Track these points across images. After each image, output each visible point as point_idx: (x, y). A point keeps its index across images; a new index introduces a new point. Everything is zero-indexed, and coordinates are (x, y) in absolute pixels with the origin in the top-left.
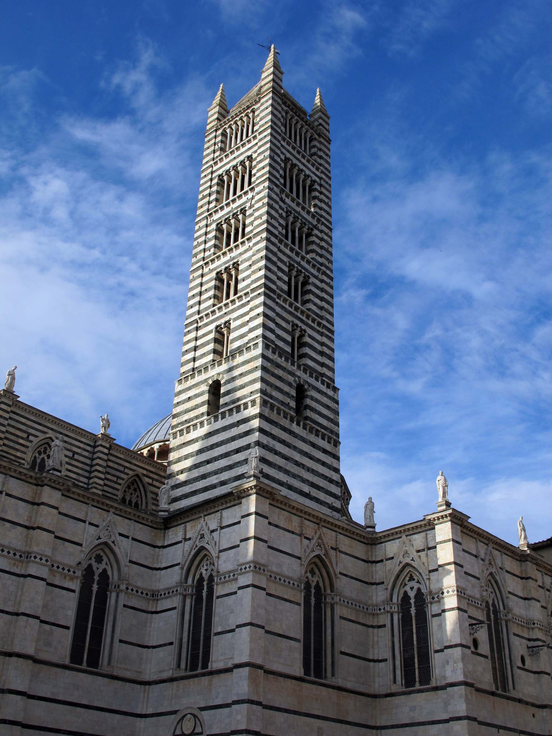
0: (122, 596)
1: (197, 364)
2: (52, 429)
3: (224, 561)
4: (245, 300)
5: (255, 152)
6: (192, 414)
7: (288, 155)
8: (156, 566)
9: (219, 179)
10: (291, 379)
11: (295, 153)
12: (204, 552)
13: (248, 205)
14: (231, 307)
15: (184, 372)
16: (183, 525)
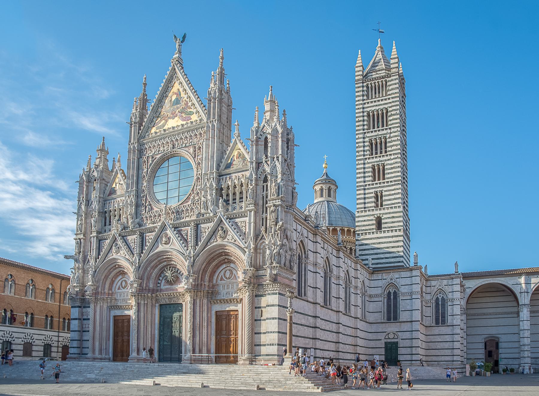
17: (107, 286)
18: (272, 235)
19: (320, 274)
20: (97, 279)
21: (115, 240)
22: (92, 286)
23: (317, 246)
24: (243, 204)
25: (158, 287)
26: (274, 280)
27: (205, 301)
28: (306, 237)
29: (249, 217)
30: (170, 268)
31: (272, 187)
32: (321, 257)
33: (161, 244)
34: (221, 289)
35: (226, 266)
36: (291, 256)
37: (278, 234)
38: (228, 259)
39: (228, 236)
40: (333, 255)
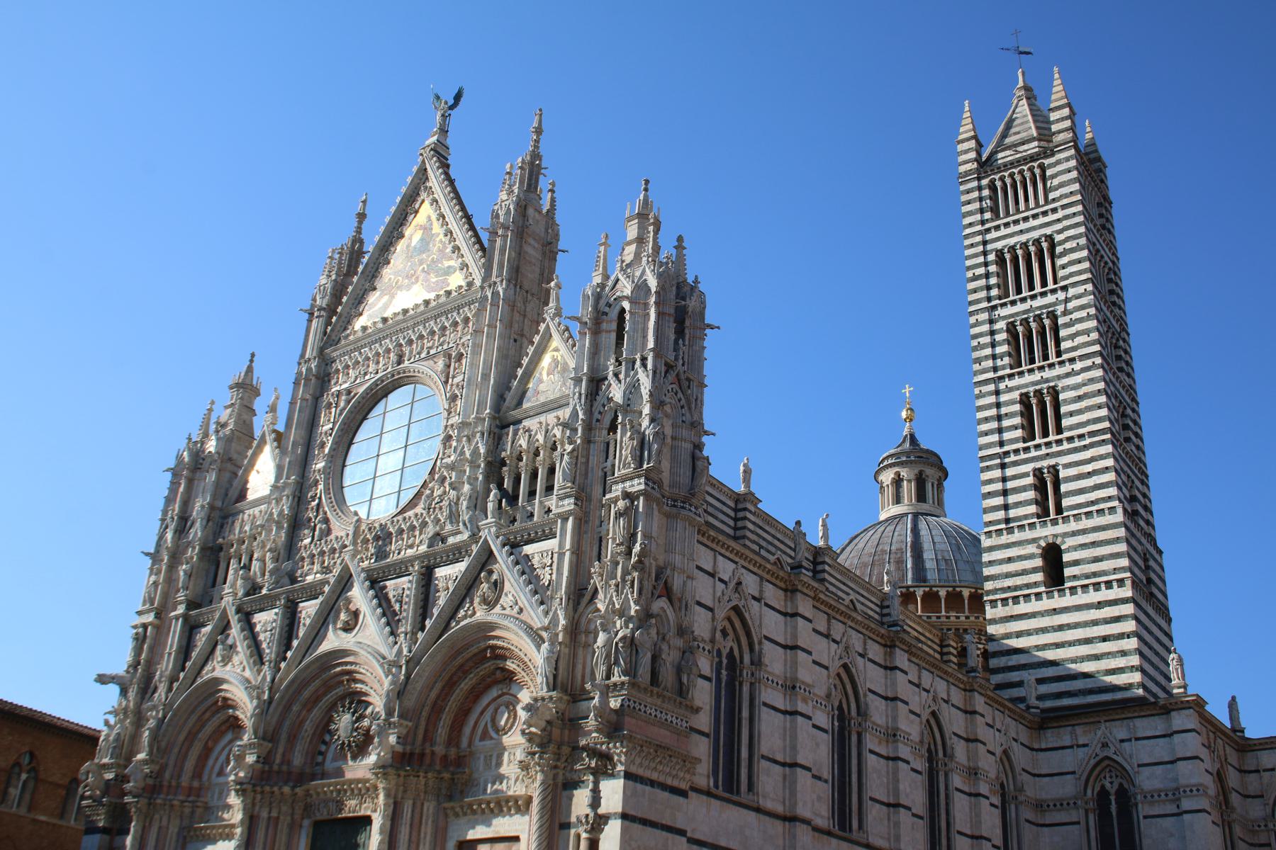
0: (1022, 808)
1: (1012, 513)
2: (852, 589)
3: (1148, 778)
4: (1077, 444)
5: (1060, 232)
6: (1019, 581)
7: (1095, 240)
8: (1036, 772)
9: (997, 256)
10: (1139, 548)
11: (1095, 231)
12: (1107, 762)
13: (1060, 309)
14: (1055, 449)
15: (990, 522)
16: (1070, 728)
17: (189, 765)
18: (617, 586)
19: (809, 718)
20: (163, 744)
21: (224, 627)
22: (147, 764)
23: (795, 628)
24: (552, 502)
25: (318, 764)
26: (613, 726)
27: (429, 807)
28: (754, 598)
29: (561, 535)
30: (351, 703)
31: (624, 443)
32: (814, 662)
33: (335, 629)
34: (481, 768)
35: (500, 692)
36: (684, 652)
37: (633, 582)
38: (504, 670)
39: (503, 596)
40: (870, 660)
